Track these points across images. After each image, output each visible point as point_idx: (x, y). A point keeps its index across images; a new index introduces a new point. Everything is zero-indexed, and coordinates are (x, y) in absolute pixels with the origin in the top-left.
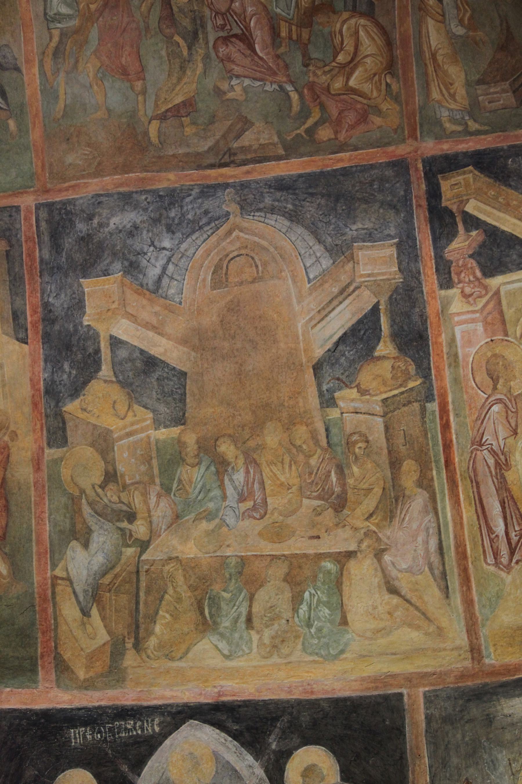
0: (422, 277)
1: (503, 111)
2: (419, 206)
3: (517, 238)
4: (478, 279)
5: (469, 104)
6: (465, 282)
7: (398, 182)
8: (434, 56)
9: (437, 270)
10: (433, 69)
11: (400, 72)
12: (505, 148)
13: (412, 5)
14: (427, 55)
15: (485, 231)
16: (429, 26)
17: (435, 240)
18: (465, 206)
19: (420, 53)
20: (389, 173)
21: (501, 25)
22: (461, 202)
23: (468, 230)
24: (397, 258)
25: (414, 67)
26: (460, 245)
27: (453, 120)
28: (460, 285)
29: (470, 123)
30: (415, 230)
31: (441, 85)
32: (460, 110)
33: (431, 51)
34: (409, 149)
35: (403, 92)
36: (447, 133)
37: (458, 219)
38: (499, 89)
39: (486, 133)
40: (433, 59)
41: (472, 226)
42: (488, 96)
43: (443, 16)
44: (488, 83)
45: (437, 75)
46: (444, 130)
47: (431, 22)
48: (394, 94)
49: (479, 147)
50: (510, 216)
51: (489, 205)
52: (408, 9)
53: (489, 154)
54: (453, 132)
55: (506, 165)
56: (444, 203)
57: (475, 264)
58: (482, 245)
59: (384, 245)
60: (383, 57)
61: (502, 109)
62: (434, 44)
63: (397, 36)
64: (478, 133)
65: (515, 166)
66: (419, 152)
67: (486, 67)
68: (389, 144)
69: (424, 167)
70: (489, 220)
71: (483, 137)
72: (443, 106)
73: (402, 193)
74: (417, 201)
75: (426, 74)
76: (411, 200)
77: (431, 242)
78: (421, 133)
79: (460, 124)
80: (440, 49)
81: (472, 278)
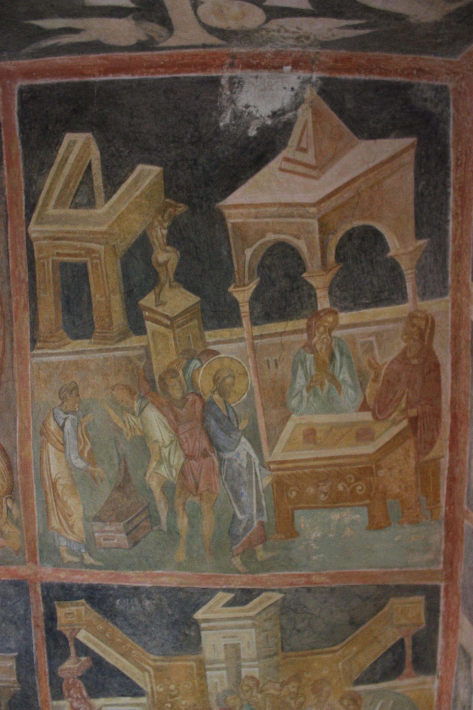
0: (38, 688)
1: (116, 550)
2: (37, 626)
3: (119, 671)
4: (83, 697)
5: (86, 539)
6: (73, 698)
7: (18, 601)
8: (54, 485)
9: (51, 684)
10: (53, 498)
11: (21, 497)
12: (116, 587)
13: (34, 428)
14: (48, 483)
15: (92, 659)
16: (50, 453)
17: (50, 658)
18: (76, 634)
19: (41, 480)
20: (11, 591)
21: (119, 465)
22: (74, 630)
23: (78, 655)
24: (17, 669)
25: (35, 494)
26: (72, 666)
27: (71, 552)
28: (70, 699)
29: (86, 556)
30: (32, 646)
31: (61, 516)
32: (77, 542)
33: (51, 479)
34: (29, 572)
35: (23, 518)
36: (66, 561)
37: (71, 644)
38: (113, 529)
39: (100, 568)
40: (53, 489)
41: (82, 651)
42: (103, 534)
43: (64, 445)
44: (103, 521)
45: (56, 505)
46: (62, 559)
47: (52, 449)
48: (15, 518)
49: (93, 581)
50: (115, 650)
51: (97, 638)
52: (29, 432)
53: (100, 590)
54: (69, 562)
55: (114, 605)
56: (59, 628)
57: (82, 685)
58: (89, 671)
59: (5, 657)
60: (4, 481)
61: (116, 548)
62: (54, 472)
63: (17, 461)
64: (92, 567)
65: (122, 607)
66: (38, 576)
67: (103, 504)
68: (11, 563)
69: (43, 591)
70: (97, 650)
71: (97, 571)
72: (61, 536)
73: (22, 612)
74: (35, 622)
75: (46, 502)
76: (30, 620)
77: (46, 659)
78: (41, 558)
79: (76, 555)
80: (59, 478)
81: (79, 696)
